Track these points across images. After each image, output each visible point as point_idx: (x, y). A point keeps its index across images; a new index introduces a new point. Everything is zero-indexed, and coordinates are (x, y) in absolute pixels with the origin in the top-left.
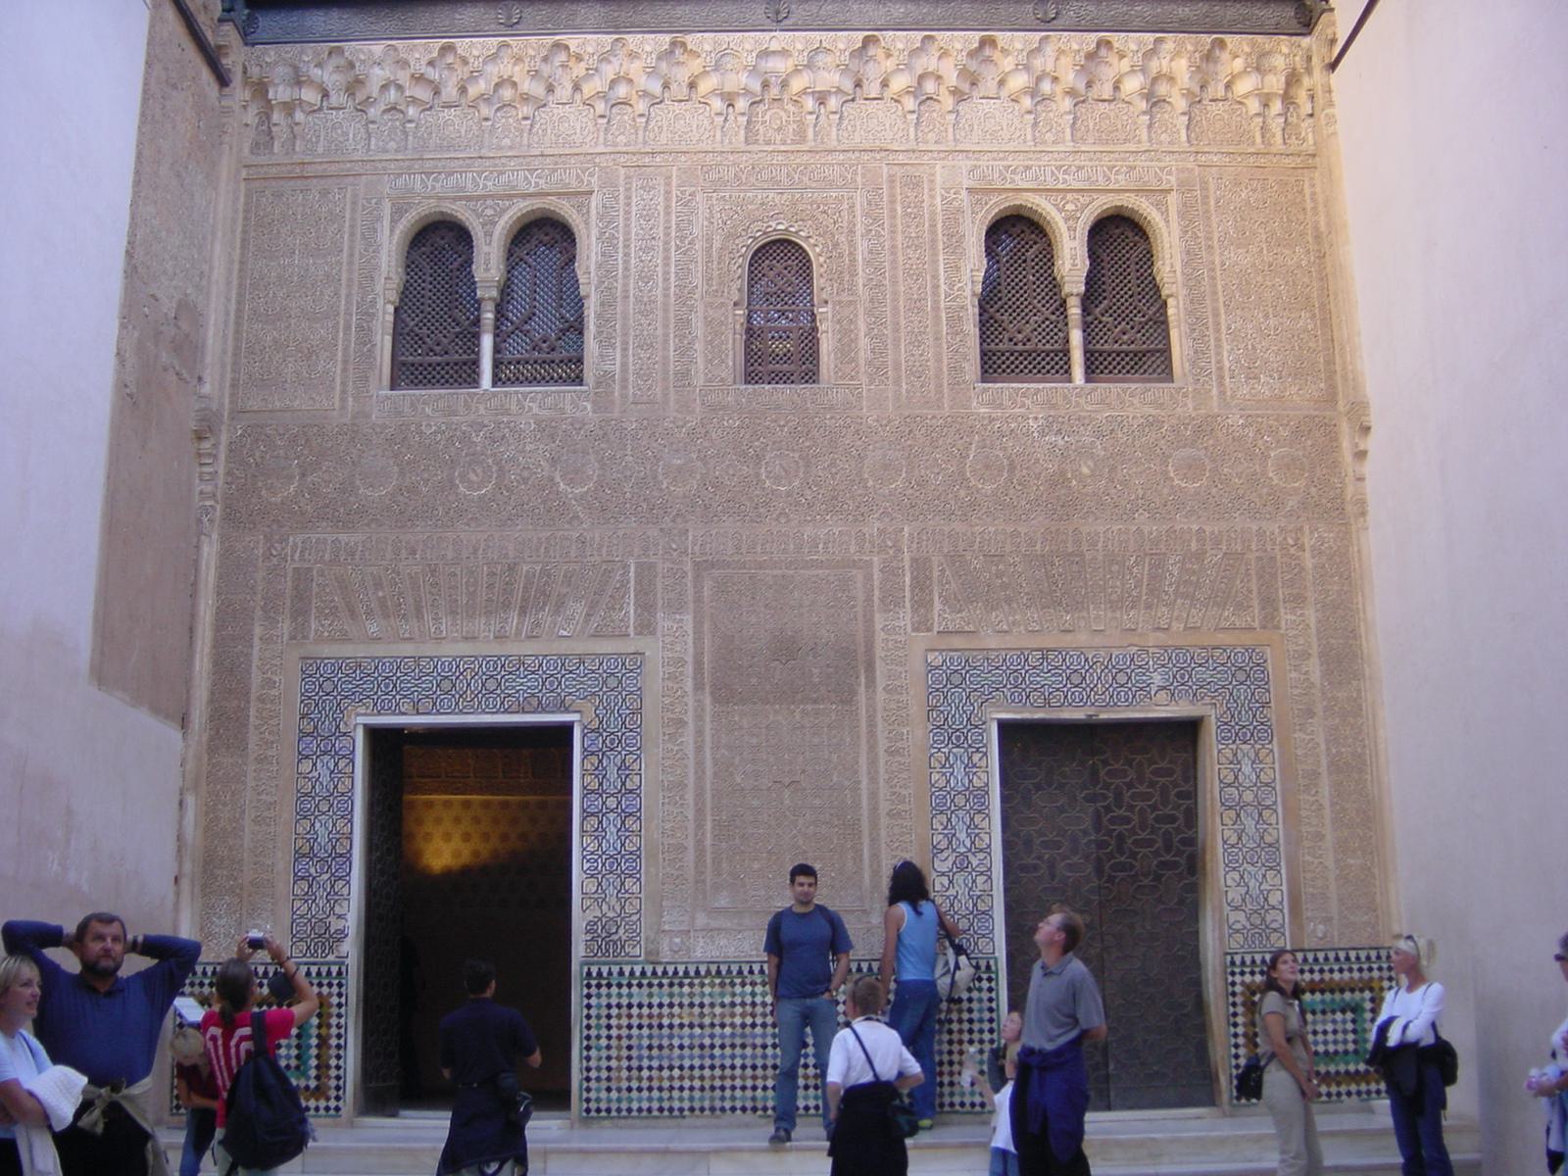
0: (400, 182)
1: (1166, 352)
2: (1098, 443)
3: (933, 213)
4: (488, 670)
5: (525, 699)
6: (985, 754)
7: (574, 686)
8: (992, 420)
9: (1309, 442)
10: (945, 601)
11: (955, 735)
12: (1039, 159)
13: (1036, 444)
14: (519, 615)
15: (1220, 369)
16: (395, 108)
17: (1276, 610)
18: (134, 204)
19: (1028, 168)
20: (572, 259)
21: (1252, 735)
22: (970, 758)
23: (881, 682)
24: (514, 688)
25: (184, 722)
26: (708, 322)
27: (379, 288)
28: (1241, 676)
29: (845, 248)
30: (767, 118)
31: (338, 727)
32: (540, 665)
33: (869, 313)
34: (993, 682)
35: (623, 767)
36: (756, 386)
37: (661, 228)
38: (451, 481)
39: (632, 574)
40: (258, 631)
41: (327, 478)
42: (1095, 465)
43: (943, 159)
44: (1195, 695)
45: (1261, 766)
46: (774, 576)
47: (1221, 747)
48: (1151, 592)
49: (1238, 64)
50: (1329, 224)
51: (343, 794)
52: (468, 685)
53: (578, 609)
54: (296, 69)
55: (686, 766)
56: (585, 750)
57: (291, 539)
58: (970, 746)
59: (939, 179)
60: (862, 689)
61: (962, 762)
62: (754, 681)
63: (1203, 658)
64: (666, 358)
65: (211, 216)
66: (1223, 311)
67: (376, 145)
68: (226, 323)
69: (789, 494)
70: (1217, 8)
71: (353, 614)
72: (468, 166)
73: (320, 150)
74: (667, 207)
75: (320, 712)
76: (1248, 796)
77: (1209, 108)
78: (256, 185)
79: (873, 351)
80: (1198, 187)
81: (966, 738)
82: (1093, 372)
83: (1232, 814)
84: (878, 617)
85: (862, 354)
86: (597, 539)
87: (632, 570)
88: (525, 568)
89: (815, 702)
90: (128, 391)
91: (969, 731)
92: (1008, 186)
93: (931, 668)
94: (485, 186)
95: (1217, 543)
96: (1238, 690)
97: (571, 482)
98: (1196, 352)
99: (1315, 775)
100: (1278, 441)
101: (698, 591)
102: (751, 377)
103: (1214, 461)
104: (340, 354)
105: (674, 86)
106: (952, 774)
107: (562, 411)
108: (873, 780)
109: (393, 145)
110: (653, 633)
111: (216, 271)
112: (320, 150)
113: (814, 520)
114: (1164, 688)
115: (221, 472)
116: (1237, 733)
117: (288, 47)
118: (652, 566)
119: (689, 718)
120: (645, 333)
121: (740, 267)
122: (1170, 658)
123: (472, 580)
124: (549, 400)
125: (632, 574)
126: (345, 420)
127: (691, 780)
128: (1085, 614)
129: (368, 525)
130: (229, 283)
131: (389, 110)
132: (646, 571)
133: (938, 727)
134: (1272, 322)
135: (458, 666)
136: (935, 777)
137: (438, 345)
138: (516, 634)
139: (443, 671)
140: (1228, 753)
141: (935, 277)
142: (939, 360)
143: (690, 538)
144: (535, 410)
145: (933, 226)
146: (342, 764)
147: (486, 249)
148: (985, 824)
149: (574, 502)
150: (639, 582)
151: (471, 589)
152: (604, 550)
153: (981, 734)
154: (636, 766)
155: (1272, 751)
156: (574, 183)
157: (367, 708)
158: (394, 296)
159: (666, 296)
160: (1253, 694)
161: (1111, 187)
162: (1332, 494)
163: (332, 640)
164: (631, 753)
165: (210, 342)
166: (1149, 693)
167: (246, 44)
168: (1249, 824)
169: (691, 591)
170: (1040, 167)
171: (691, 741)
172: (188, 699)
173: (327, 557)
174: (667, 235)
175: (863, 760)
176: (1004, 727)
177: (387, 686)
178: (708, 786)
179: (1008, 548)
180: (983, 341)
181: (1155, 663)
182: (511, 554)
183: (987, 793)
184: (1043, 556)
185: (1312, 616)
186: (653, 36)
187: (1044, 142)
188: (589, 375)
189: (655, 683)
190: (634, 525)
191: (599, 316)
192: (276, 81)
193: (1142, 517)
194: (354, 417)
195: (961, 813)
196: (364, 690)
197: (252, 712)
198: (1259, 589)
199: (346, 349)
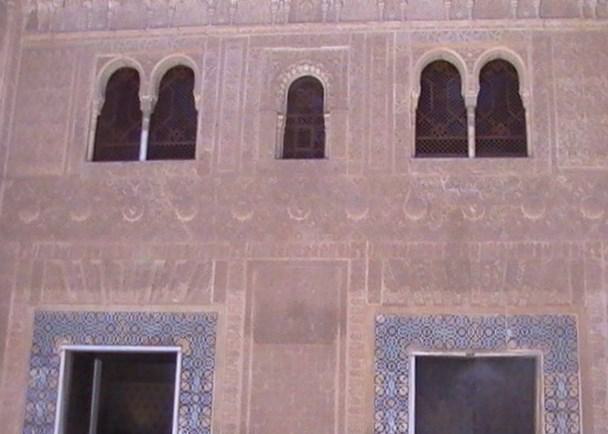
1: (524, 141)
3: (391, 61)
6: (407, 376)
8: (419, 179)
10: (387, 287)
11: (389, 364)
14: (153, 290)
15: (554, 149)
19: (446, 33)
22: (398, 378)
27: (88, 105)
30: (302, 7)
35: (203, 378)
39: (214, 268)
53: (184, 287)
57: (34, 245)
59: (395, 41)
60: (338, 336)
66: (556, 114)
69: (302, 222)
76: (562, 405)
83: (552, 415)
84: (349, 294)
93: (378, 324)
101: (250, 279)
108: (342, 389)
114: (512, 339)
116: (555, 367)
119: (241, 352)
121: (283, 91)
125: (214, 268)
127: (240, 387)
132: (221, 266)
134: (585, 120)
136: (378, 388)
140: (552, 380)
141: (391, 95)
144: (167, 173)
148: (405, 418)
154: (210, 378)
155: (577, 378)
158: (96, 113)
168: (562, 422)
169: (245, 279)
175: (337, 377)
176: (418, 359)
189: (223, 331)
195: (391, 411)
199: (69, 138)
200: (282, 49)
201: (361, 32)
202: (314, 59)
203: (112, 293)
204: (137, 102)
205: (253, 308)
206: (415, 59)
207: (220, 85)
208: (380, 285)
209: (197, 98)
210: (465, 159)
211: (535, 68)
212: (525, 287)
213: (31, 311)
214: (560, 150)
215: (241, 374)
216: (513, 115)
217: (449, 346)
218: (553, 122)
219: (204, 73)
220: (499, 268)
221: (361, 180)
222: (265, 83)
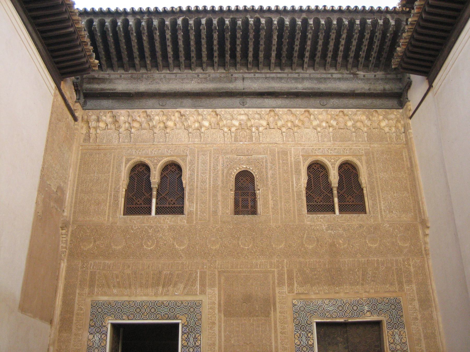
0: (129, 152)
2: (344, 233)
3: (291, 163)
4: (152, 305)
5: (164, 315)
6: (312, 333)
7: (180, 311)
8: (311, 226)
9: (410, 232)
12: (322, 146)
13: (325, 233)
15: (381, 209)
16: (128, 130)
17: (403, 285)
18: (45, 155)
19: (320, 149)
20: (181, 176)
21: (398, 326)
22: (307, 335)
23: (278, 310)
24: (160, 311)
25: (51, 322)
26: (223, 196)
27: (121, 184)
28: (393, 307)
29: (265, 173)
30: (241, 134)
31: (102, 324)
32: (169, 304)
33: (272, 193)
34: (314, 310)
35: (195, 338)
36: (237, 216)
37: (208, 167)
38: (142, 244)
39: (198, 275)
40: (78, 291)
41: (102, 242)
42: (344, 240)
43: (294, 146)
44: (379, 313)
45: (402, 337)
46: (243, 275)
47: (388, 330)
48: (363, 280)
49: (381, 117)
50: (412, 165)
51: (103, 347)
52: (145, 310)
53: (181, 286)
54: (98, 118)
55: (215, 338)
56: (183, 332)
58: (307, 331)
59: (293, 151)
61: (305, 336)
62: (237, 309)
63: (381, 301)
64: (209, 206)
65: (70, 160)
67: (122, 140)
68: (73, 194)
69: (248, 249)
70: (374, 101)
71: (109, 287)
72: (149, 147)
73: (104, 142)
74: (210, 160)
75: (97, 319)
77: (373, 131)
78: (85, 151)
79: (274, 204)
80: (371, 155)
81: (306, 328)
82: (341, 210)
84: (276, 288)
85: (270, 206)
86: (188, 263)
87: (199, 273)
88: (164, 272)
89: (257, 316)
90: (39, 214)
91: (307, 326)
92: (314, 154)
93: (294, 305)
94: (154, 153)
95: (383, 264)
96: (393, 312)
97: (180, 245)
98: (373, 204)
99: (419, 340)
100: (400, 231)
101: (220, 281)
102: (237, 212)
103: (381, 238)
104: (108, 204)
105: (213, 124)
106: (302, 340)
107: (177, 223)
108: (276, 342)
109: (127, 140)
110: (205, 294)
111: (70, 178)
112: (104, 142)
113: (256, 258)
115: (69, 240)
117: (96, 111)
118: (205, 272)
119: (217, 322)
120: (203, 199)
122: (370, 301)
123: (147, 276)
124: (173, 219)
125: (198, 275)
126: (109, 224)
128: (342, 287)
129: (115, 258)
130: (74, 181)
131: (126, 130)
133: (297, 325)
134: (395, 195)
135: (142, 304)
136: (296, 341)
137: (139, 201)
138: (161, 294)
139: (137, 305)
140: (391, 333)
141: (292, 182)
142: (294, 207)
143: (217, 263)
144: (169, 222)
145: (291, 166)
146: (103, 336)
147: (154, 172)
149: (180, 252)
150: (201, 277)
151: (147, 279)
152: (190, 267)
153: (310, 327)
154: (199, 338)
155: (405, 332)
156: (182, 153)
157: (112, 317)
158: (125, 187)
159: (210, 187)
160: (397, 313)
161: (345, 154)
162: (418, 248)
163: (102, 295)
164: (198, 333)
165: (67, 199)
166: (364, 313)
167: (83, 109)
170: (323, 149)
171: (217, 330)
172: (53, 314)
173: (101, 268)
174: (210, 169)
175: (273, 335)
176: (318, 324)
177: (119, 310)
178: (223, 345)
179: (317, 266)
180: (307, 202)
181: (365, 303)
182: (160, 268)
183: (313, 346)
184: (329, 269)
185: (414, 287)
186: (206, 109)
187: (324, 141)
188: (186, 211)
189: (205, 310)
190: (199, 259)
191: (189, 193)
192: (92, 121)
193: (359, 255)
194: (112, 224)
196: (111, 311)
197: (74, 318)
198: (397, 279)
199: (110, 203)
200: (231, 156)
201: (274, 148)
202: (249, 162)
203: (139, 290)
204: (149, 182)
205: (222, 298)
206: (304, 162)
207: (198, 175)
208: (294, 283)
209: (184, 182)
210: (335, 215)
211: (368, 168)
212: (372, 283)
213: (89, 300)
214: (384, 210)
215: (217, 333)
216: (356, 192)
217: (334, 316)
218: (379, 195)
219: (188, 168)
220: (358, 273)
221: (279, 226)
222: (223, 174)
